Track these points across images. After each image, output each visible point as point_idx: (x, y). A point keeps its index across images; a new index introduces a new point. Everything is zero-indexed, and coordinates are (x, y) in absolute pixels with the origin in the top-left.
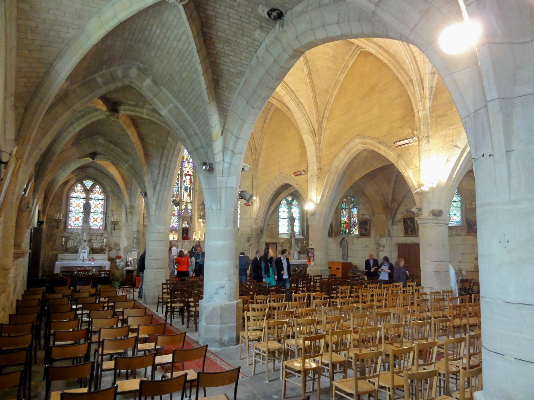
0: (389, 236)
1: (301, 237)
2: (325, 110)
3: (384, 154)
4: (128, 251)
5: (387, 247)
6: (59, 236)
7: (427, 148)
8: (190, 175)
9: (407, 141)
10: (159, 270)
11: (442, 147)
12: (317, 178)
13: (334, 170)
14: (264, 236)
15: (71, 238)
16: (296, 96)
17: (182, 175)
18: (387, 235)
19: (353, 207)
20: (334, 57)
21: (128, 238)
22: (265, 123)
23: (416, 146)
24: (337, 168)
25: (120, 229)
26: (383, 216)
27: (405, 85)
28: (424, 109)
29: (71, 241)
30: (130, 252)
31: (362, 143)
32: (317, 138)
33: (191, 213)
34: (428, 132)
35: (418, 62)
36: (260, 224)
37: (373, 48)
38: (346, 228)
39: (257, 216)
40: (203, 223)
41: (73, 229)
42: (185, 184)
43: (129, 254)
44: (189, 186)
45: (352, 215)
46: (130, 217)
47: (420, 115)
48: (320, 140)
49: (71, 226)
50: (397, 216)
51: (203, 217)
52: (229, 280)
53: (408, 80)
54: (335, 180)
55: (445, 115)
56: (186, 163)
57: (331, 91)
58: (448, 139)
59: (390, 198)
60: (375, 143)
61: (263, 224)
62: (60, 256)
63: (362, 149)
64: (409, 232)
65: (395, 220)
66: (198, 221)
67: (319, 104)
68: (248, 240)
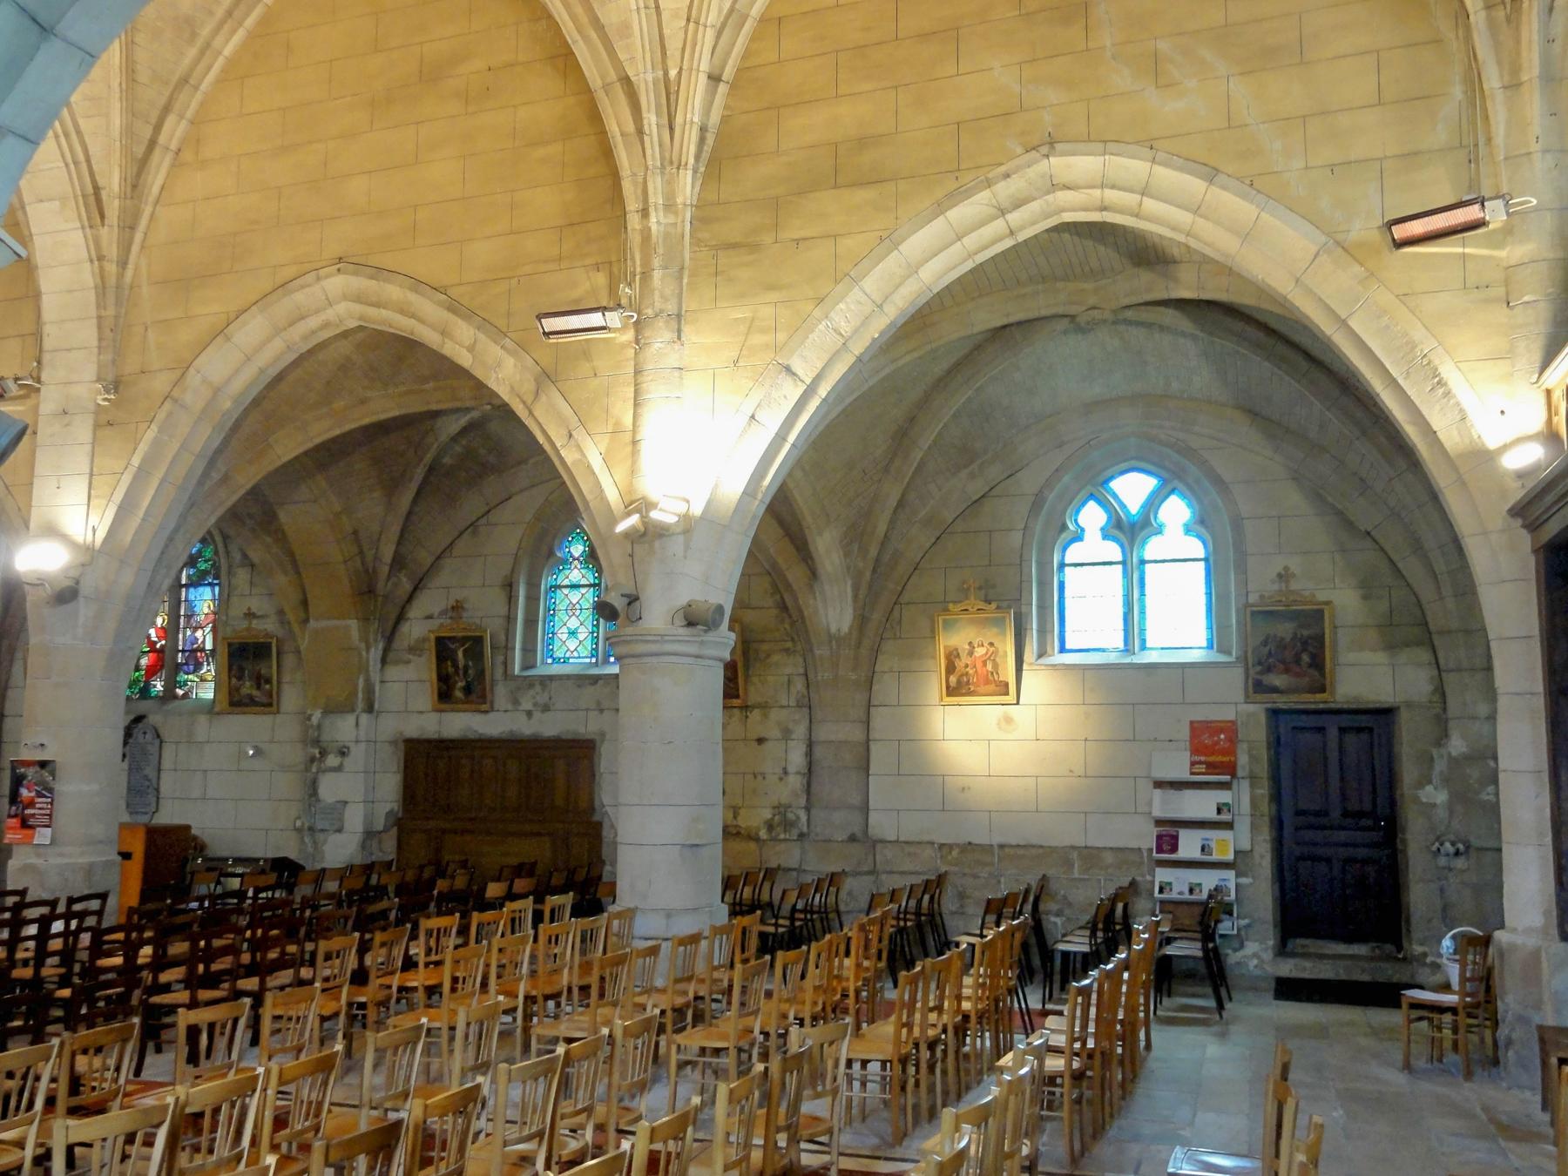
0: (370, 709)
2: (166, 110)
3: (465, 359)
5: (358, 753)
7: (673, 360)
9: (595, 319)
11: (736, 363)
12: (97, 426)
13: (194, 395)
18: (360, 705)
19: (193, 584)
23: (624, 346)
24: (217, 391)
26: (353, 624)
27: (600, 95)
28: (669, 206)
31: (359, 299)
32: (109, 235)
35: (665, 16)
38: (152, 671)
45: (189, 617)
47: (654, 228)
48: (125, 247)
50: (405, 628)
53: (612, 75)
54: (197, 446)
55: (754, 248)
57: (205, 32)
58: (757, 339)
59: (388, 552)
60: (429, 307)
63: (352, 324)
64: (458, 694)
65: (396, 644)
67: (143, 76)
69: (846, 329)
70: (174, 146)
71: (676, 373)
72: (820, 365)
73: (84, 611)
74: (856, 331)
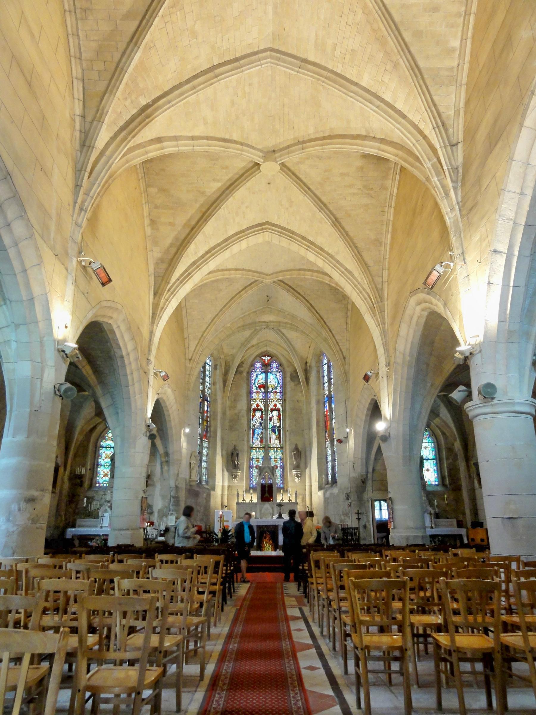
1: (440, 489)
4: (163, 514)
6: (82, 496)
8: (278, 410)
10: (122, 532)
13: (399, 360)
14: (369, 488)
15: (96, 498)
16: (338, 262)
17: (267, 410)
20: (365, 187)
21: (163, 497)
22: (347, 317)
25: (154, 485)
28: (452, 210)
29: (95, 503)
30: (166, 516)
33: (283, 462)
34: (462, 244)
36: (360, 470)
37: (371, 147)
39: (354, 457)
40: (298, 477)
41: (102, 487)
42: (272, 423)
43: (165, 519)
44: (278, 425)
46: (165, 468)
49: (99, 484)
51: (297, 467)
52: (8, 520)
54: (405, 376)
56: (272, 394)
61: (364, 470)
62: (79, 522)
66: (291, 474)
67: (370, 263)
68: (348, 497)
69: (512, 215)
70: (386, 280)
71: (467, 279)
72: (508, 240)
73: (393, 443)
74: (517, 213)
